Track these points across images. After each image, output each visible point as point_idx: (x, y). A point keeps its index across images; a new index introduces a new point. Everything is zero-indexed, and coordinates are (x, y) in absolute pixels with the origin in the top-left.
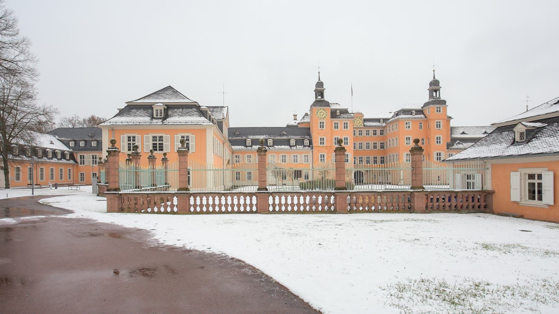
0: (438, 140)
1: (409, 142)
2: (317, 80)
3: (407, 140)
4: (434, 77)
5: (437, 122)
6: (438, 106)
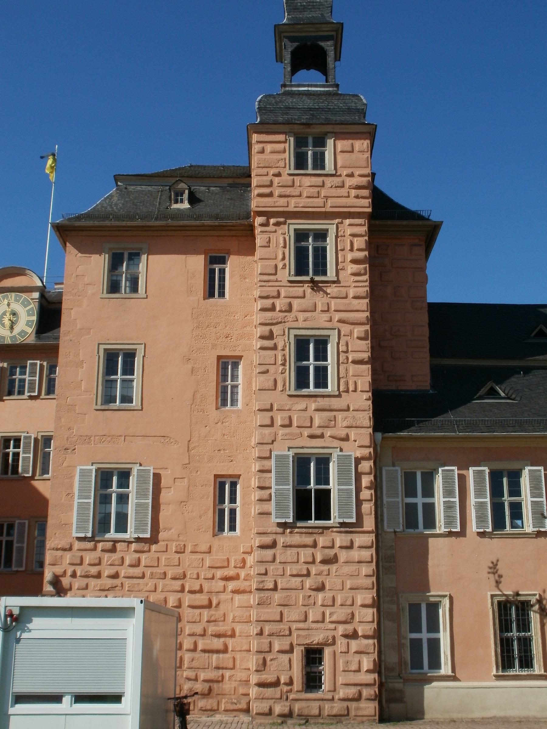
1: (127, 384)
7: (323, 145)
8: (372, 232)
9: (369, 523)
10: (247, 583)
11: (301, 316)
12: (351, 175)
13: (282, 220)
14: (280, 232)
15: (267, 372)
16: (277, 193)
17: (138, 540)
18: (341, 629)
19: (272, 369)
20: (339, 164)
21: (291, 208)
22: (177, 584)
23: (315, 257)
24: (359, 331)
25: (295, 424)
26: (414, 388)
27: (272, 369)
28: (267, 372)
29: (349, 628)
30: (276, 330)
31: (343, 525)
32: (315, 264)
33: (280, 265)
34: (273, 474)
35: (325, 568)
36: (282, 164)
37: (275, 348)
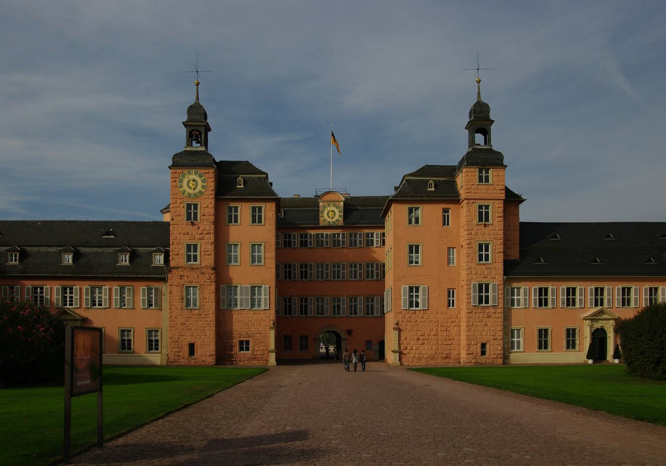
0: (484, 253)
1: (417, 257)
3: (411, 251)
4: (479, 94)
9: (501, 305)
11: (481, 237)
14: (473, 206)
19: (471, 255)
20: (494, 180)
25: (479, 273)
26: (514, 259)
27: (471, 255)
33: (474, 218)
35: (487, 319)
36: (474, 181)
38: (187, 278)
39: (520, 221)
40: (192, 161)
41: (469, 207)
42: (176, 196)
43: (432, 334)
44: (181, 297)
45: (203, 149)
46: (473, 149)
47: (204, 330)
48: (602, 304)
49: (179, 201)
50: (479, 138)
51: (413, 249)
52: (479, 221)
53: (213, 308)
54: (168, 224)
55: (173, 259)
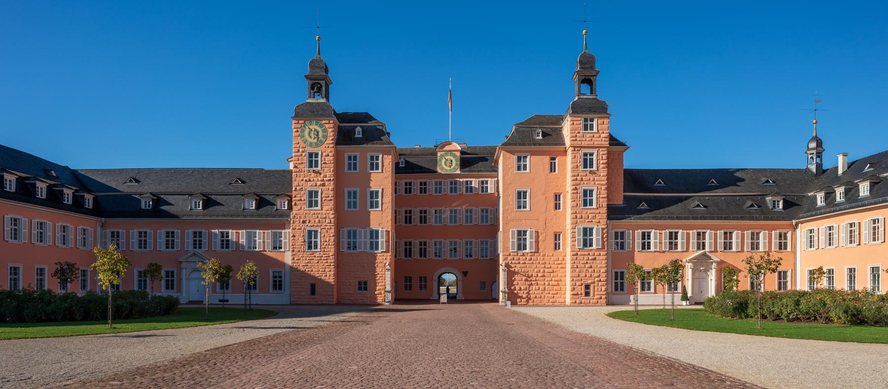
2: (315, 56)
3: (519, 197)
5: (585, 155)
6: (589, 116)
7: (593, 121)
8: (609, 154)
10: (564, 265)
12: (603, 133)
13: (579, 149)
15: (575, 201)
16: (578, 140)
17: (531, 252)
18: (596, 279)
19: (576, 200)
21: (583, 145)
22: (543, 266)
23: (590, 162)
24: (603, 188)
27: (576, 200)
28: (575, 201)
29: (599, 279)
30: (578, 187)
31: (598, 249)
32: (590, 165)
33: (579, 165)
34: (576, 234)
37: (577, 193)
38: (309, 222)
39: (624, 168)
40: (313, 112)
41: (574, 155)
42: (298, 146)
43: (539, 275)
44: (303, 240)
45: (323, 100)
46: (579, 98)
47: (325, 271)
48: (704, 248)
49: (301, 150)
50: (585, 88)
51: (521, 195)
52: (584, 168)
53: (333, 250)
54: (290, 172)
55: (295, 204)
